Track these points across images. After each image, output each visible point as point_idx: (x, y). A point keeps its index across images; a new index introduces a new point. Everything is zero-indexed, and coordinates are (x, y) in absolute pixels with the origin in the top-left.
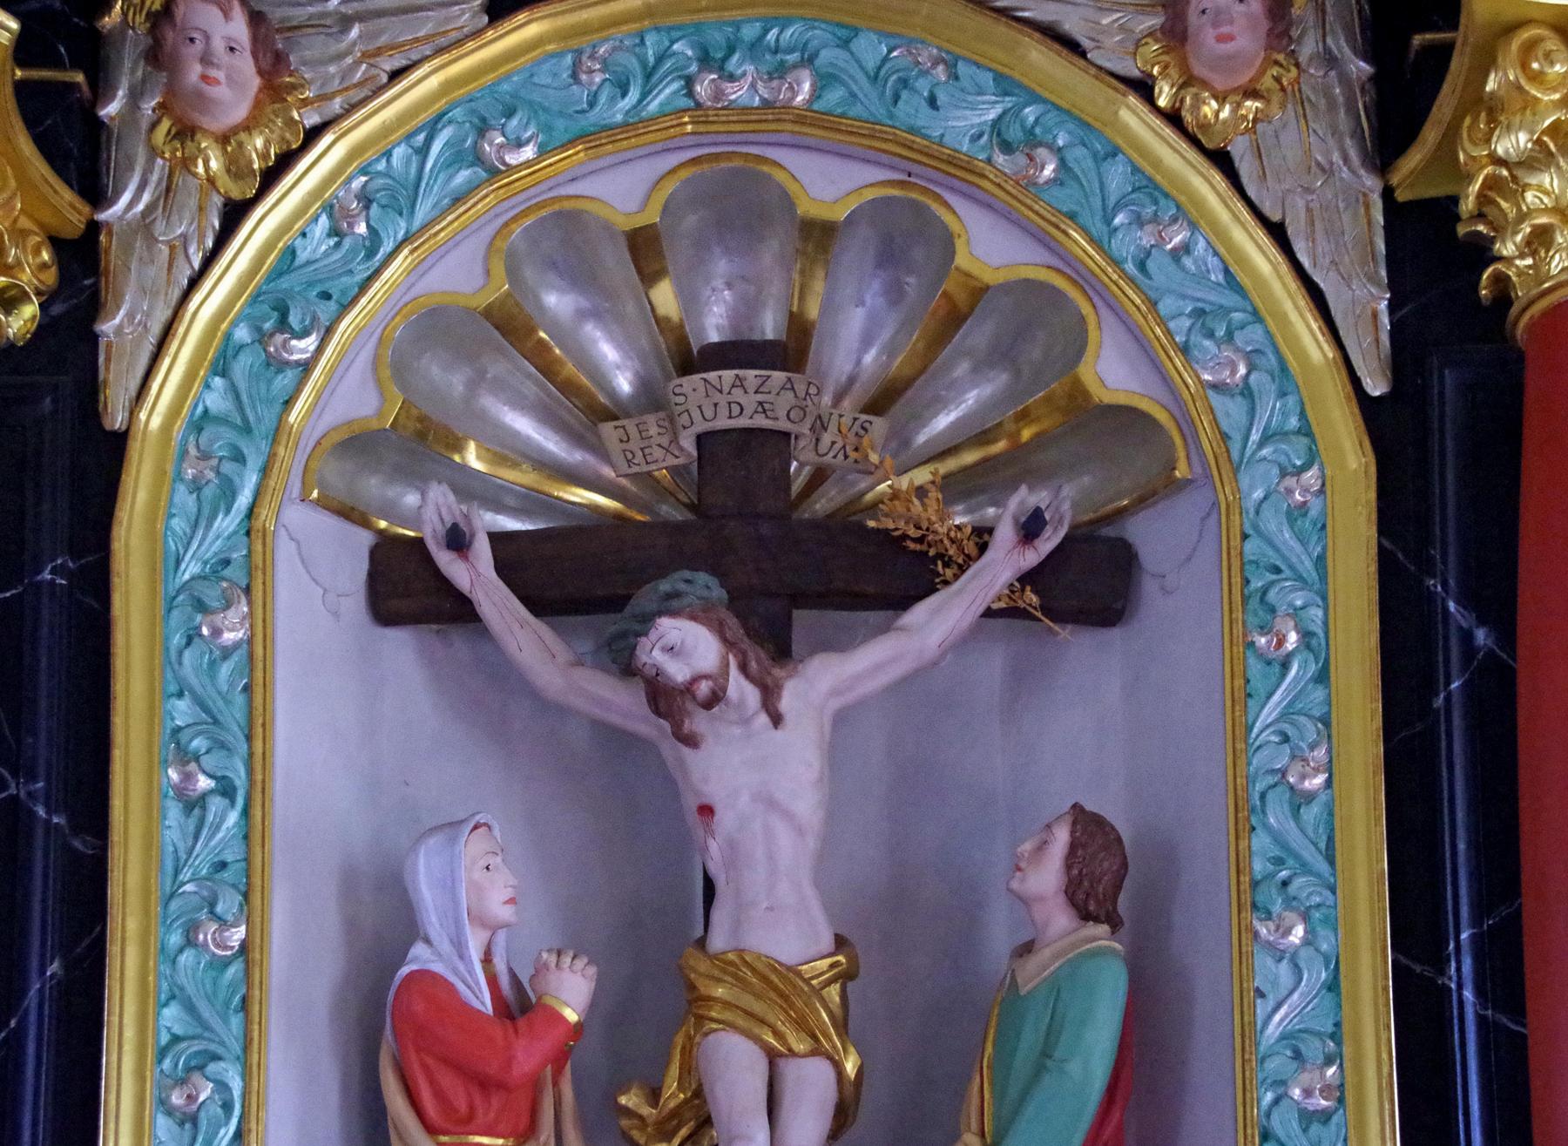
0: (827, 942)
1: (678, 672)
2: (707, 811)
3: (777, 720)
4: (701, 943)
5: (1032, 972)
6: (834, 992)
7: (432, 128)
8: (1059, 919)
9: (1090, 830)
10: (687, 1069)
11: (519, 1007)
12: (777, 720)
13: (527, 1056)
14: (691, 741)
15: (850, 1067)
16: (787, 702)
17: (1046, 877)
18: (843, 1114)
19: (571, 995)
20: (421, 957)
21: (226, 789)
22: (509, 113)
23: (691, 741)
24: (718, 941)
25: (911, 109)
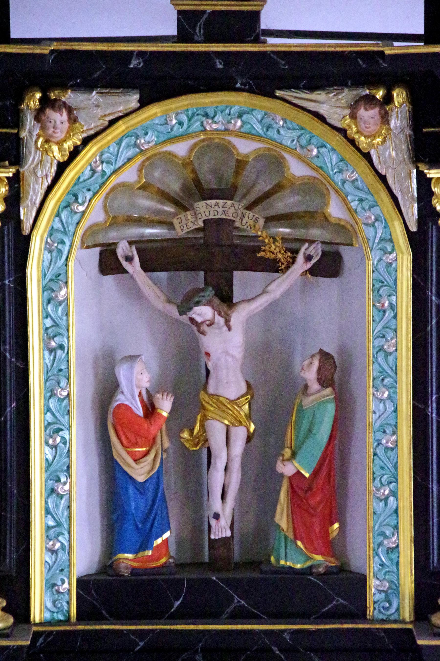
0: (243, 388)
1: (199, 319)
2: (208, 354)
3: (229, 329)
4: (205, 387)
5: (308, 402)
6: (247, 406)
7: (121, 140)
8: (315, 386)
9: (325, 356)
10: (202, 426)
11: (150, 410)
12: (229, 329)
13: (153, 429)
14: (203, 333)
15: (252, 427)
16: (233, 322)
17: (311, 375)
18: (249, 439)
19: (165, 406)
20: (120, 399)
21: (61, 347)
22: (146, 134)
23: (203, 333)
24: (211, 390)
25: (272, 133)
